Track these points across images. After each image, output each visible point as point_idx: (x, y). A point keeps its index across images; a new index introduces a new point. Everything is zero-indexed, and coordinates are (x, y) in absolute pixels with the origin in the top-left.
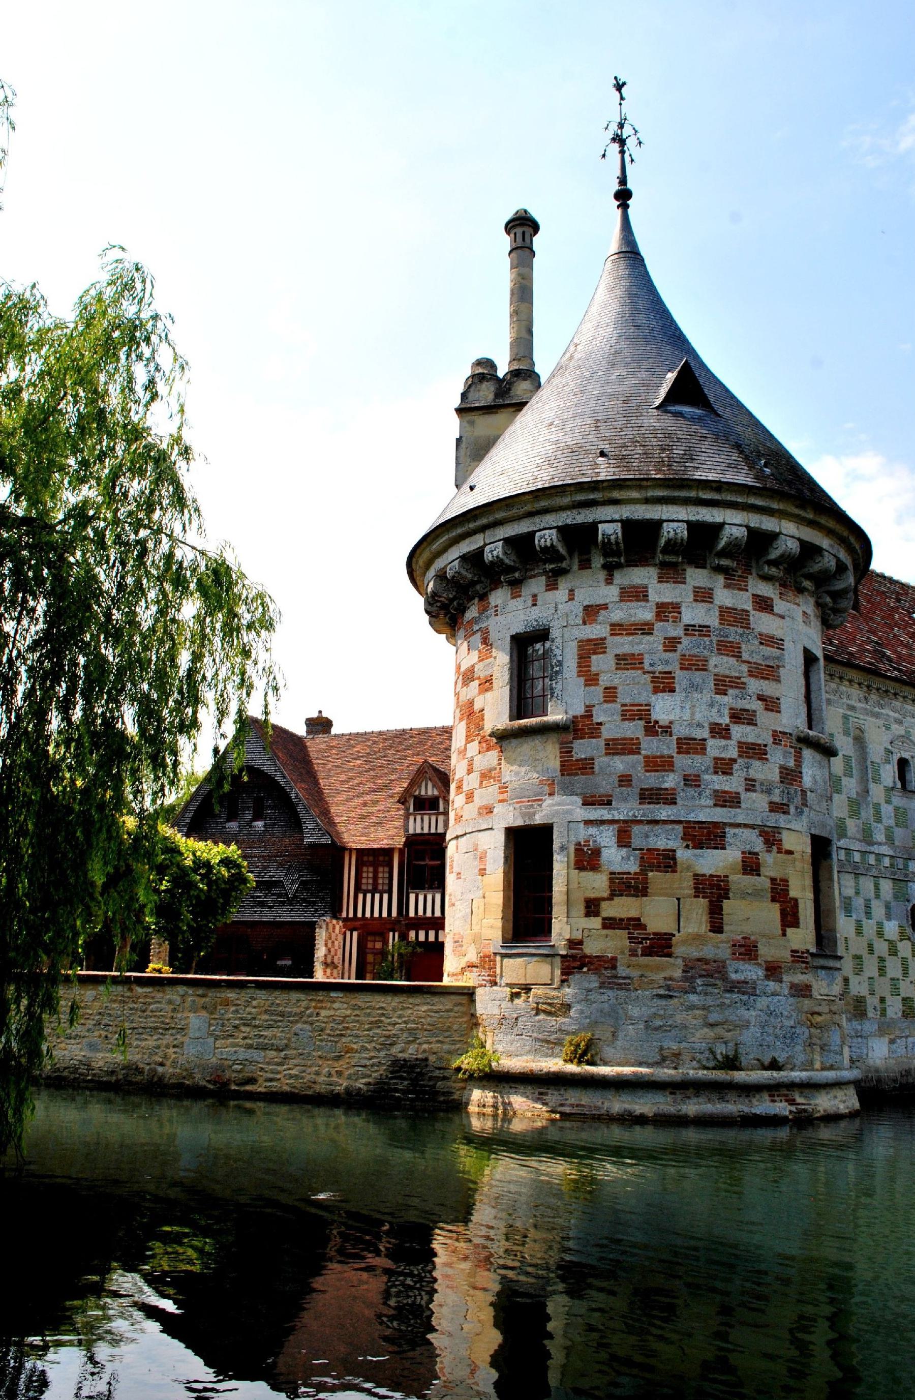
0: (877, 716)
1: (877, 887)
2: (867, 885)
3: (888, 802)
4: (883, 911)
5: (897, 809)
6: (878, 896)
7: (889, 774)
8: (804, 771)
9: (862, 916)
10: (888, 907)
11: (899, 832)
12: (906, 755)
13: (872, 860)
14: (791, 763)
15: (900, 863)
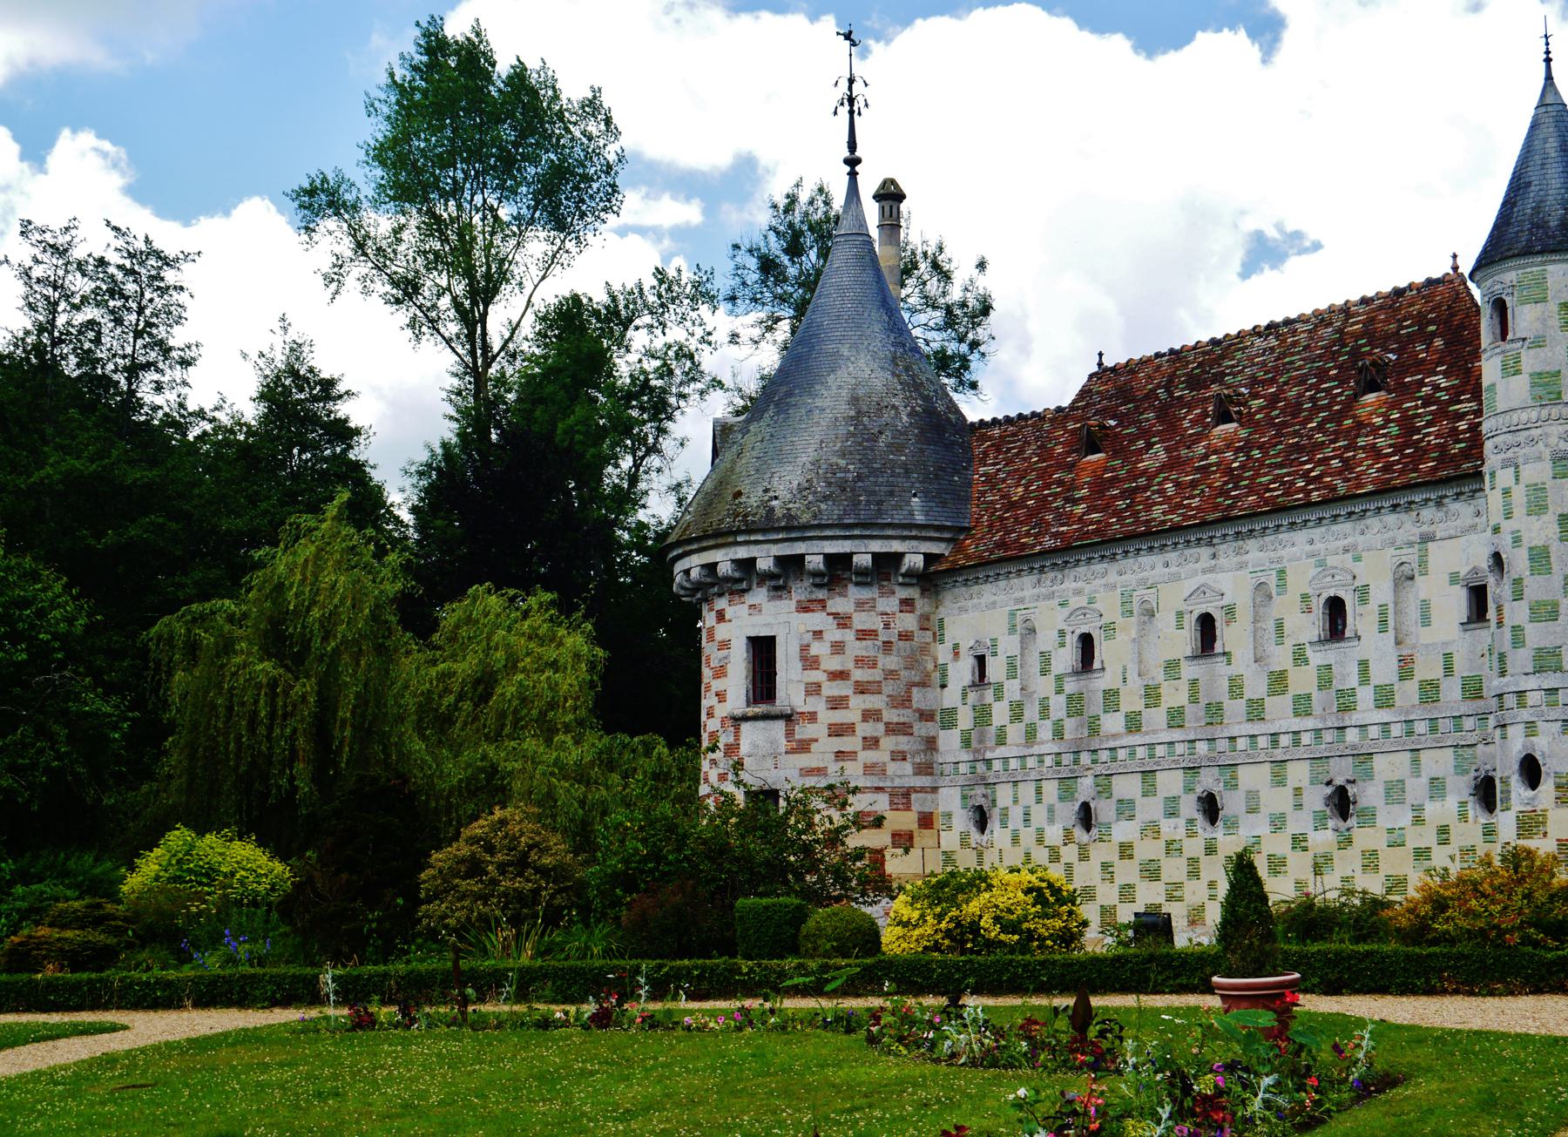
0: (1051, 596)
1: (1039, 792)
2: (1026, 791)
3: (1059, 691)
4: (1045, 814)
5: (1070, 697)
6: (1039, 801)
7: (1066, 658)
8: (741, 742)
9: (1020, 825)
10: (1051, 810)
11: (1070, 725)
12: (1084, 629)
13: (1031, 763)
14: (731, 740)
15: (1067, 759)
